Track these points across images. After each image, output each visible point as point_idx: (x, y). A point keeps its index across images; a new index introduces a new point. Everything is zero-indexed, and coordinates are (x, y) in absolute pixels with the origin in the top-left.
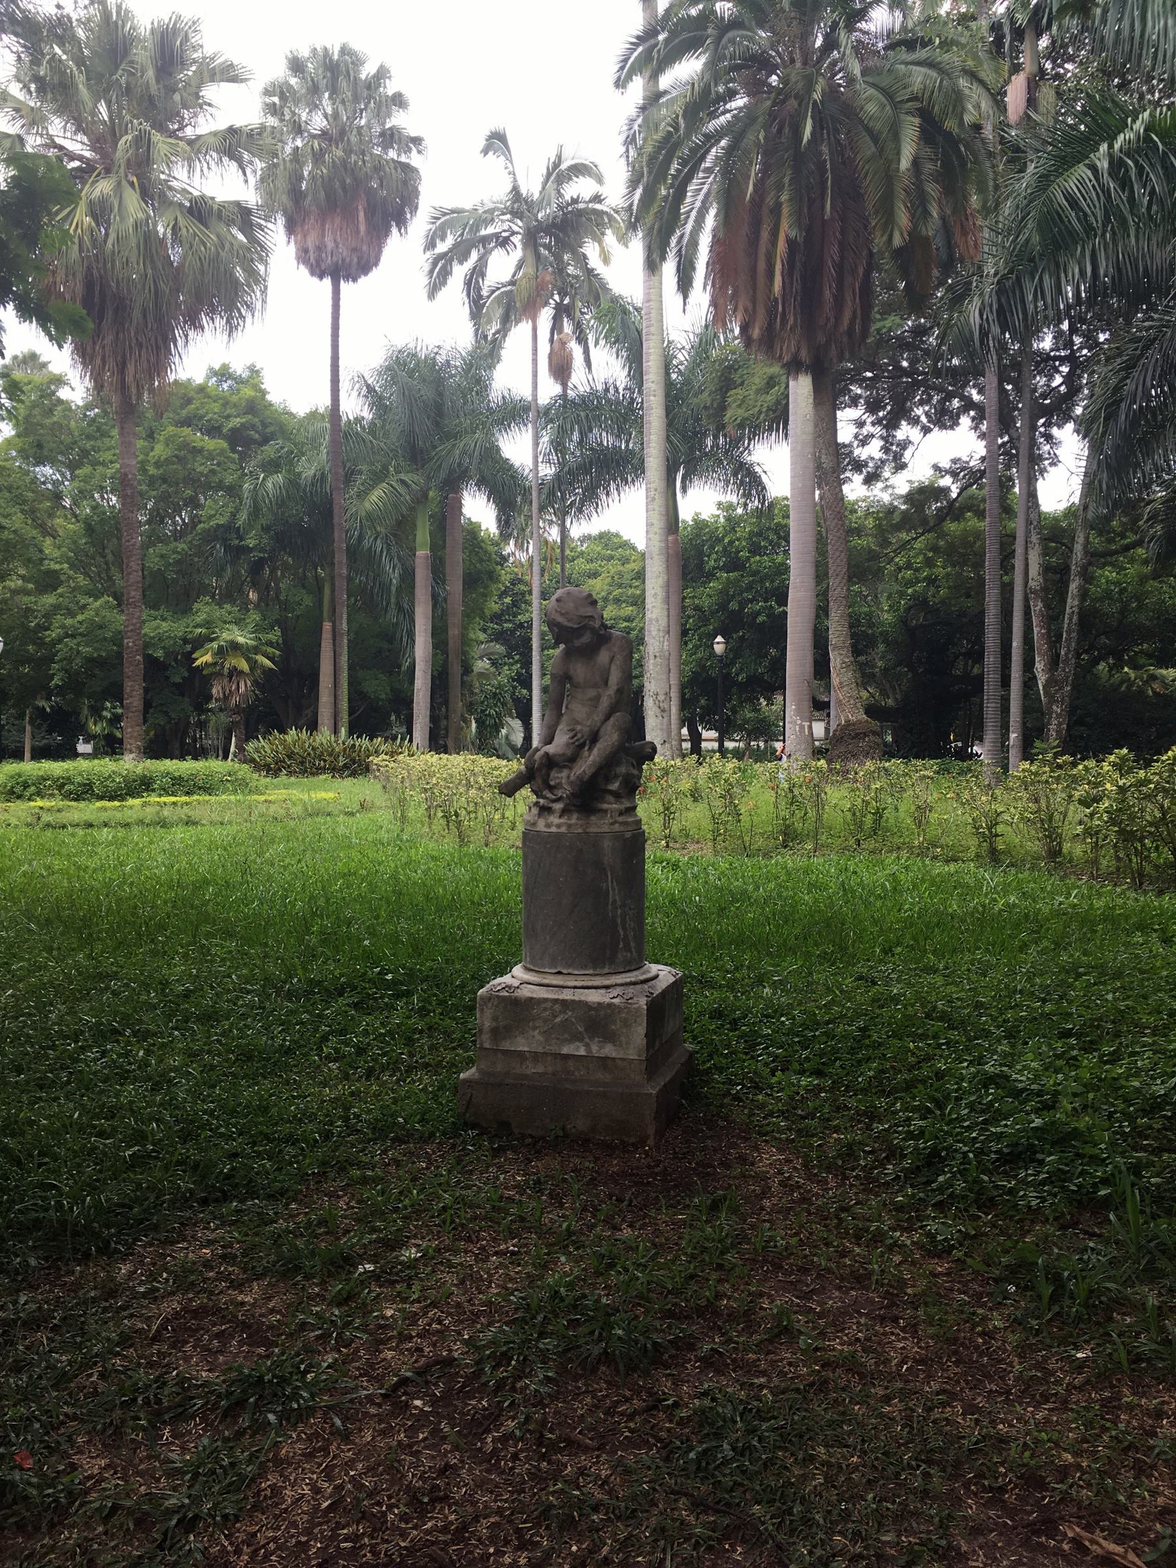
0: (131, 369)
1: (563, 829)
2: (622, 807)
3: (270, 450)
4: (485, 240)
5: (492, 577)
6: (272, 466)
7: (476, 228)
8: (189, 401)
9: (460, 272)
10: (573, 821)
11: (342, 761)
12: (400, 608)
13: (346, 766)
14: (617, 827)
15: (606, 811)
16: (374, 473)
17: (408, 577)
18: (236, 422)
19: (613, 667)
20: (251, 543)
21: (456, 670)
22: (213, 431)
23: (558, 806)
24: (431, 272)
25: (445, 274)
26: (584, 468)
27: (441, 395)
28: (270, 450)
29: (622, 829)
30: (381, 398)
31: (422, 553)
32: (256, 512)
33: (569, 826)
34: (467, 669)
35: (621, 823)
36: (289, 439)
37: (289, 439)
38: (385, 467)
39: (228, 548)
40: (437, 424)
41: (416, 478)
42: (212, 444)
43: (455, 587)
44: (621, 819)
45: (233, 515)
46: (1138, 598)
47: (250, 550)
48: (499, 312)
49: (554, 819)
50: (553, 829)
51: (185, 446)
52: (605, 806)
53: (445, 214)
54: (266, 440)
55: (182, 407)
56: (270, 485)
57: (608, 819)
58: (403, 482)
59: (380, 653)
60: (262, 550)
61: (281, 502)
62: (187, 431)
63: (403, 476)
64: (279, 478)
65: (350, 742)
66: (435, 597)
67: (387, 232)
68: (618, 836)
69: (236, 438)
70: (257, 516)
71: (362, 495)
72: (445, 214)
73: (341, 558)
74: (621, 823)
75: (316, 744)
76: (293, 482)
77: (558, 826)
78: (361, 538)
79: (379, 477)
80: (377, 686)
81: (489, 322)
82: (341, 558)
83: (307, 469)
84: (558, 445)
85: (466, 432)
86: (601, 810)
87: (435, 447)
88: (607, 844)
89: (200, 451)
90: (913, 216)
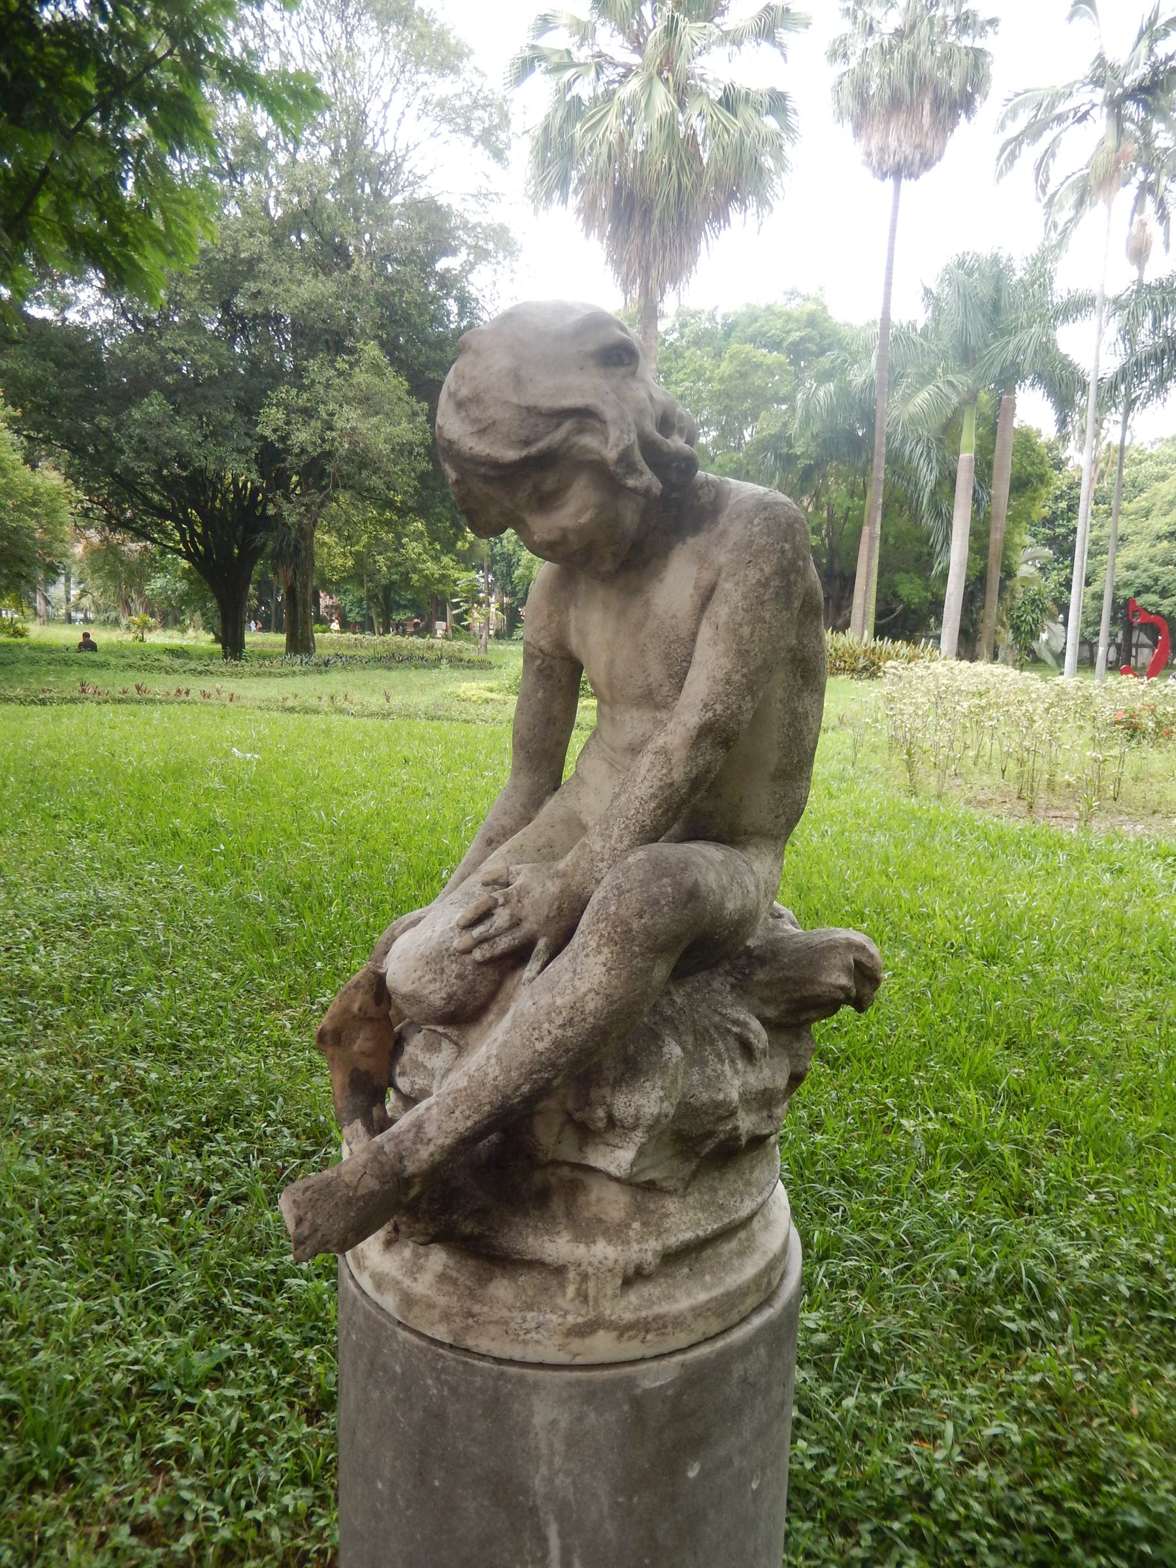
0: (654, 273)
1: (389, 1302)
2: (647, 1250)
3: (825, 362)
4: (1060, 118)
5: (1042, 479)
6: (824, 377)
7: (1052, 106)
8: (756, 320)
9: (1031, 153)
10: (423, 1286)
11: (862, 663)
12: (939, 514)
13: (865, 668)
14: (603, 1345)
15: (559, 1271)
16: (922, 376)
17: (948, 479)
18: (795, 336)
19: (706, 632)
20: (798, 451)
21: (995, 575)
22: (775, 345)
24: (999, 158)
25: (1013, 157)
26: (1156, 357)
27: (998, 290)
28: (825, 362)
29: (632, 1348)
30: (938, 299)
31: (966, 457)
32: (807, 420)
33: (408, 1301)
34: (1009, 573)
35: (623, 1330)
36: (845, 349)
37: (845, 349)
38: (934, 370)
39: (778, 456)
40: (991, 321)
41: (964, 378)
42: (774, 357)
43: (1001, 488)
44: (629, 1307)
45: (785, 425)
47: (797, 457)
48: (1072, 199)
51: (747, 361)
52: (558, 1247)
53: (1017, 95)
54: (822, 352)
55: (750, 325)
56: (821, 393)
57: (565, 1310)
58: (950, 383)
59: (912, 555)
60: (810, 457)
61: (831, 412)
62: (749, 347)
63: (950, 378)
64: (831, 387)
65: (872, 644)
66: (976, 500)
67: (955, 123)
68: (599, 1386)
69: (797, 352)
70: (808, 423)
71: (907, 398)
72: (1017, 95)
73: (880, 462)
74: (642, 1327)
75: (838, 645)
76: (844, 391)
77: (380, 1281)
78: (904, 441)
79: (925, 379)
80: (910, 590)
81: (1061, 208)
82: (880, 462)
83: (858, 377)
84: (1129, 334)
85: (1022, 328)
86: (537, 1265)
87: (987, 346)
88: (545, 1416)
89: (758, 366)
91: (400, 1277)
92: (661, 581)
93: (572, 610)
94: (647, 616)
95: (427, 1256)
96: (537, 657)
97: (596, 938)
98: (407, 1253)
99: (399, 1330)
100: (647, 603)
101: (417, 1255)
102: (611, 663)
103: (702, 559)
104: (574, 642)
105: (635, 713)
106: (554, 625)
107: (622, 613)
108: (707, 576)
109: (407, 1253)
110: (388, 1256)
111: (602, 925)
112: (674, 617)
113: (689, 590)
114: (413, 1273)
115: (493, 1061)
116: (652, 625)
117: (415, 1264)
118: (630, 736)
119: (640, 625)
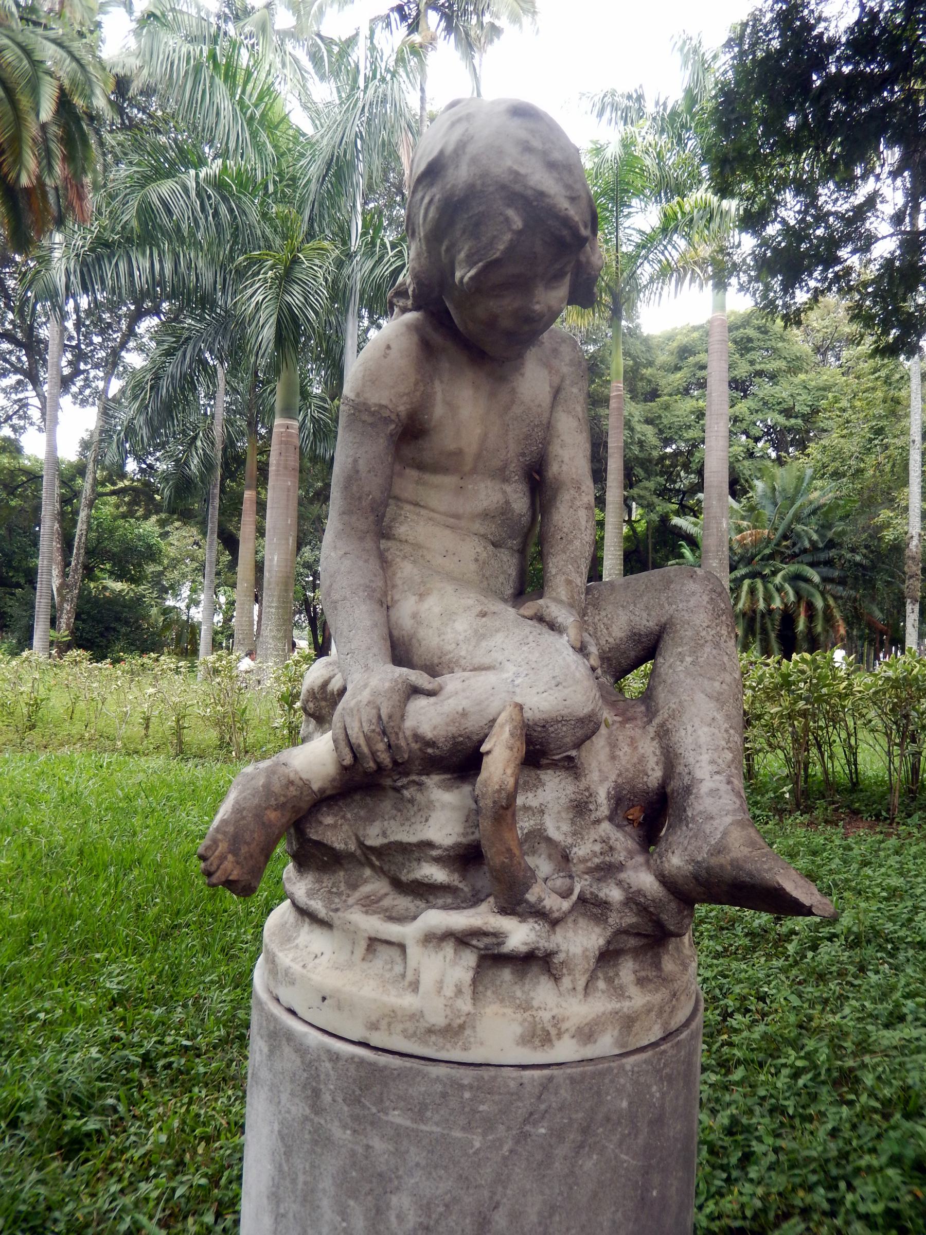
23: (580, 941)
33: (628, 1022)
46: (111, 532)
49: (568, 1005)
50: (566, 1050)
90: (39, 163)
91: (618, 1006)
92: (522, 375)
93: (437, 383)
94: (513, 402)
95: (617, 975)
96: (392, 421)
97: (724, 627)
98: (601, 984)
99: (624, 1060)
100: (513, 391)
101: (610, 981)
102: (484, 438)
103: (548, 366)
104: (439, 411)
105: (489, 483)
106: (418, 394)
107: (492, 395)
108: (556, 380)
109: (601, 984)
110: (590, 999)
111: (724, 618)
112: (540, 406)
113: (548, 389)
114: (622, 995)
115: (732, 731)
116: (517, 410)
117: (615, 989)
118: (485, 504)
119: (507, 408)
